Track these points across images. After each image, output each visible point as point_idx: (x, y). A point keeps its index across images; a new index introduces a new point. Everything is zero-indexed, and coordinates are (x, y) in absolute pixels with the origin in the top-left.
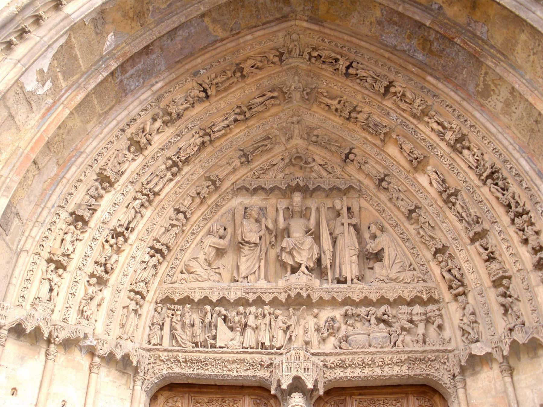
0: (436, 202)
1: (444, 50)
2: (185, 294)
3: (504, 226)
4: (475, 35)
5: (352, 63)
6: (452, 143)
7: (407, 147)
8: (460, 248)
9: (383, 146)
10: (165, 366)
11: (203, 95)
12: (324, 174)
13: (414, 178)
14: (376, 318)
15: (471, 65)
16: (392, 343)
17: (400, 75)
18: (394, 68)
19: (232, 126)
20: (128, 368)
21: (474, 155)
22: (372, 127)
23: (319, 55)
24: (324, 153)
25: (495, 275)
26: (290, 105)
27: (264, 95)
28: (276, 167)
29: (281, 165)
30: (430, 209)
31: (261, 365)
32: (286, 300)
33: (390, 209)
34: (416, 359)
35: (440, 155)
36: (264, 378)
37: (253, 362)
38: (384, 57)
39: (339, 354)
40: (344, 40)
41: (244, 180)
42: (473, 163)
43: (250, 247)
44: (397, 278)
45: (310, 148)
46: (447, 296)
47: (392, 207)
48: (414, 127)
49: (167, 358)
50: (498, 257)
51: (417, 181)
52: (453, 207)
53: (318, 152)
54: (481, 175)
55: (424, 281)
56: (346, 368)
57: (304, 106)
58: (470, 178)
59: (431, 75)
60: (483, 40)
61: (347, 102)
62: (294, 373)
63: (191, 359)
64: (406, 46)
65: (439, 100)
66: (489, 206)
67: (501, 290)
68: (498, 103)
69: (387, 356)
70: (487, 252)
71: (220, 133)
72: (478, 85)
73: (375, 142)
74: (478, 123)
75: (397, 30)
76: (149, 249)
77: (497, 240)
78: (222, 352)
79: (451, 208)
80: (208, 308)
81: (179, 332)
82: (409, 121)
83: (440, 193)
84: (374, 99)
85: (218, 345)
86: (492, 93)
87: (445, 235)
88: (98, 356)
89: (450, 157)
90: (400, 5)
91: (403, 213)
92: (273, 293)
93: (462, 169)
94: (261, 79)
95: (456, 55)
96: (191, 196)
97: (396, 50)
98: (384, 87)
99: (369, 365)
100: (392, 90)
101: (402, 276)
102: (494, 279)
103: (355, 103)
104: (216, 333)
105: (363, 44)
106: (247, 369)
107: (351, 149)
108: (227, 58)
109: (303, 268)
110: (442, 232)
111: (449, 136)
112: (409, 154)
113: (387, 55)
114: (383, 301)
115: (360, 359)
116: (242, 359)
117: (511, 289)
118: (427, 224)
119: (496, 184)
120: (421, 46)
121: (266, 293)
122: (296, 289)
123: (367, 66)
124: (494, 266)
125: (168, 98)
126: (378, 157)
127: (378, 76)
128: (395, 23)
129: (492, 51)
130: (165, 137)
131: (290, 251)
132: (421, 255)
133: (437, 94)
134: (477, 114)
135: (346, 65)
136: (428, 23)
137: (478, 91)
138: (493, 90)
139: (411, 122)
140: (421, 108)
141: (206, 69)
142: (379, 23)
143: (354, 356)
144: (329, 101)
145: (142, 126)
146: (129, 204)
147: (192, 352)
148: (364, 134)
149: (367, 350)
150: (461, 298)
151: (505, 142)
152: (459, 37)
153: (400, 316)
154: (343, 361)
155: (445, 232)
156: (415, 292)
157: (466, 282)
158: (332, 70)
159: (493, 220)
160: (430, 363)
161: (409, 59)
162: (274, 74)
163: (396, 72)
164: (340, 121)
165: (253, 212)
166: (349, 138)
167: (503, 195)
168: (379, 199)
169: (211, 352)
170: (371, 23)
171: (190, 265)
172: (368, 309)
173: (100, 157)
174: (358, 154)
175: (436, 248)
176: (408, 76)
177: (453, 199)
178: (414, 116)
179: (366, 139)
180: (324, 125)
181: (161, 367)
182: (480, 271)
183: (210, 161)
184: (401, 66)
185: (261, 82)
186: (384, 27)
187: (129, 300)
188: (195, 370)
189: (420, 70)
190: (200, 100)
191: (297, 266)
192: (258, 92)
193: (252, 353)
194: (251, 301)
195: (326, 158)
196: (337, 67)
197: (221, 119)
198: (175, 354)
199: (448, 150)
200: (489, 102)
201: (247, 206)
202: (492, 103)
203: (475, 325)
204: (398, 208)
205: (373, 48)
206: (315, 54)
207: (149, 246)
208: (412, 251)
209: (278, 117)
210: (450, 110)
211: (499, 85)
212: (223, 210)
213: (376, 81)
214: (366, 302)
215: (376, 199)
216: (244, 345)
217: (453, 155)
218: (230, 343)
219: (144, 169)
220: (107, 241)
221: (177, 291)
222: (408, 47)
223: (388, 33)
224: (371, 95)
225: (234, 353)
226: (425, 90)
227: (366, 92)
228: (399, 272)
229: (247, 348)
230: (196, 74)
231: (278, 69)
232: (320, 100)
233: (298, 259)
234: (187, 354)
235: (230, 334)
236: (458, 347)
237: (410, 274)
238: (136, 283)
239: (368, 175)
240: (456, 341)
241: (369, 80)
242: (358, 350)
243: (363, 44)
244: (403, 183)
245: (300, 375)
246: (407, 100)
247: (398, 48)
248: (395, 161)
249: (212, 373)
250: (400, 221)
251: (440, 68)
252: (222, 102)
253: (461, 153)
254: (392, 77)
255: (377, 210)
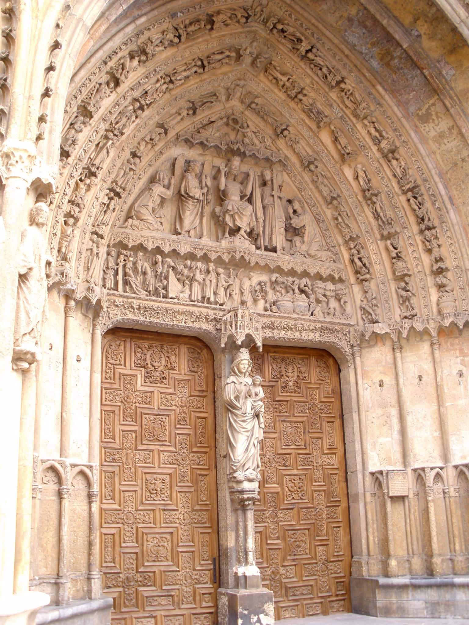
0: (356, 196)
1: (402, 68)
2: (138, 242)
3: (413, 233)
4: (441, 73)
5: (312, 47)
6: (386, 151)
7: (343, 141)
8: (371, 241)
9: (318, 132)
10: (119, 312)
11: (176, 40)
12: (257, 142)
13: (341, 170)
14: (299, 288)
15: (422, 92)
16: (310, 313)
17: (352, 74)
18: (349, 66)
19: (191, 78)
20: (89, 312)
21: (400, 167)
22: (315, 113)
23: (282, 29)
24: (258, 120)
25: (401, 272)
26: (239, 68)
27: (222, 53)
28: (215, 125)
29: (219, 124)
30: (350, 201)
31: (206, 318)
32: (230, 260)
33: (311, 190)
34: (327, 328)
35: (370, 157)
36: (208, 331)
37: (200, 315)
38: (344, 53)
39: (270, 316)
40: (310, 22)
41: (186, 132)
42: (399, 173)
43: (193, 202)
44: (316, 255)
45: (247, 113)
46: (353, 280)
47: (314, 190)
48: (352, 125)
49: (122, 303)
50: (404, 257)
51: (343, 173)
52: (371, 205)
53: (253, 119)
54: (402, 186)
55: (334, 261)
56: (273, 330)
57: (252, 72)
58: (392, 185)
59: (380, 84)
60: (446, 80)
61: (295, 81)
62: (247, 331)
63: (145, 307)
64: (366, 49)
65: (381, 109)
66: (403, 213)
67: (403, 284)
68: (432, 131)
69: (306, 323)
70: (397, 251)
71: (180, 82)
72: (420, 109)
73: (312, 128)
74: (410, 140)
75: (364, 33)
76: (108, 191)
77: (405, 243)
78: (174, 303)
79: (369, 205)
80: (159, 257)
81: (132, 279)
82: (349, 118)
83: (364, 191)
84: (322, 87)
85: (170, 295)
86: (431, 121)
87: (359, 226)
88: (74, 300)
89: (379, 162)
90: (385, 18)
91: (324, 198)
92: (217, 252)
93: (387, 175)
94: (224, 36)
95: (411, 77)
96: (146, 141)
97: (355, 50)
98: (337, 81)
99: (291, 329)
100: (343, 86)
101: (319, 254)
102: (399, 274)
103: (302, 85)
104: (168, 284)
105: (328, 33)
106: (194, 321)
107: (288, 126)
108: (203, 5)
109: (242, 232)
110: (357, 223)
111: (383, 144)
112: (343, 148)
113: (347, 52)
114: (305, 274)
115: (286, 323)
116: (191, 311)
117: (409, 285)
118: (345, 213)
119: (415, 198)
120: (380, 56)
121: (211, 251)
122: (240, 252)
123: (325, 56)
124: (400, 264)
125: (147, 34)
126: (311, 141)
127: (333, 68)
128: (365, 27)
129: (451, 92)
130: (136, 77)
131: (232, 215)
132: (333, 238)
133: (381, 103)
134: (413, 134)
135: (307, 49)
136: (405, 46)
137: (418, 114)
138: (433, 120)
139: (351, 120)
140: (365, 111)
141: (183, 13)
142: (350, 20)
143: (281, 320)
144: (280, 76)
145: (122, 61)
146: (99, 143)
147: (147, 300)
148: (303, 116)
149: (292, 316)
150: (366, 284)
151: (430, 166)
152: (428, 70)
153: (316, 289)
154: (273, 323)
155: (359, 224)
156: (329, 270)
157: (371, 271)
158: (290, 47)
159: (405, 225)
160: (336, 333)
161: (364, 62)
162: (235, 33)
163: (349, 70)
164: (282, 96)
165: (196, 168)
166: (287, 115)
167: (420, 208)
168: (303, 178)
169: (164, 302)
170: (341, 17)
171: (142, 211)
172: (293, 279)
173: (83, 88)
174: (291, 132)
175: (350, 236)
176: (359, 78)
177: (374, 199)
178: (356, 116)
179: (304, 121)
180: (266, 96)
181: (115, 312)
182: (386, 265)
183: (165, 108)
184: (356, 66)
185: (223, 38)
186: (352, 25)
187: (91, 242)
188: (148, 318)
189: (372, 77)
190: (172, 44)
191: (235, 228)
192: (218, 48)
193: (200, 307)
194: (199, 256)
195: (259, 127)
196: (299, 47)
197: (184, 68)
198: (130, 300)
199: (378, 155)
200: (425, 126)
201: (188, 159)
202: (427, 129)
203: (376, 308)
204: (320, 192)
205: (336, 41)
206: (280, 27)
207: (108, 187)
208: (324, 232)
209: (227, 76)
210: (389, 121)
211: (441, 118)
212: (163, 158)
213: (330, 72)
214: (292, 273)
215: (300, 178)
216: (193, 299)
217: (382, 161)
218: (181, 295)
219: (115, 107)
220: (81, 180)
221: (131, 238)
222: (367, 51)
223: (353, 32)
224: (320, 83)
225: (184, 305)
226: (372, 96)
227: (316, 79)
228: (318, 250)
229: (194, 302)
230: (173, 15)
231: (240, 30)
232: (271, 72)
233: (239, 223)
234: (141, 301)
235: (179, 286)
236: (358, 323)
237: (324, 253)
238: (98, 225)
239: (298, 155)
240: (357, 318)
241: (325, 70)
242: (285, 315)
243: (328, 33)
244: (329, 171)
245: (251, 333)
246: (352, 99)
247: (356, 48)
248: (326, 149)
249: (164, 322)
250: (319, 203)
251: (389, 81)
252: (187, 51)
253: (389, 161)
254: (344, 73)
255: (298, 188)
